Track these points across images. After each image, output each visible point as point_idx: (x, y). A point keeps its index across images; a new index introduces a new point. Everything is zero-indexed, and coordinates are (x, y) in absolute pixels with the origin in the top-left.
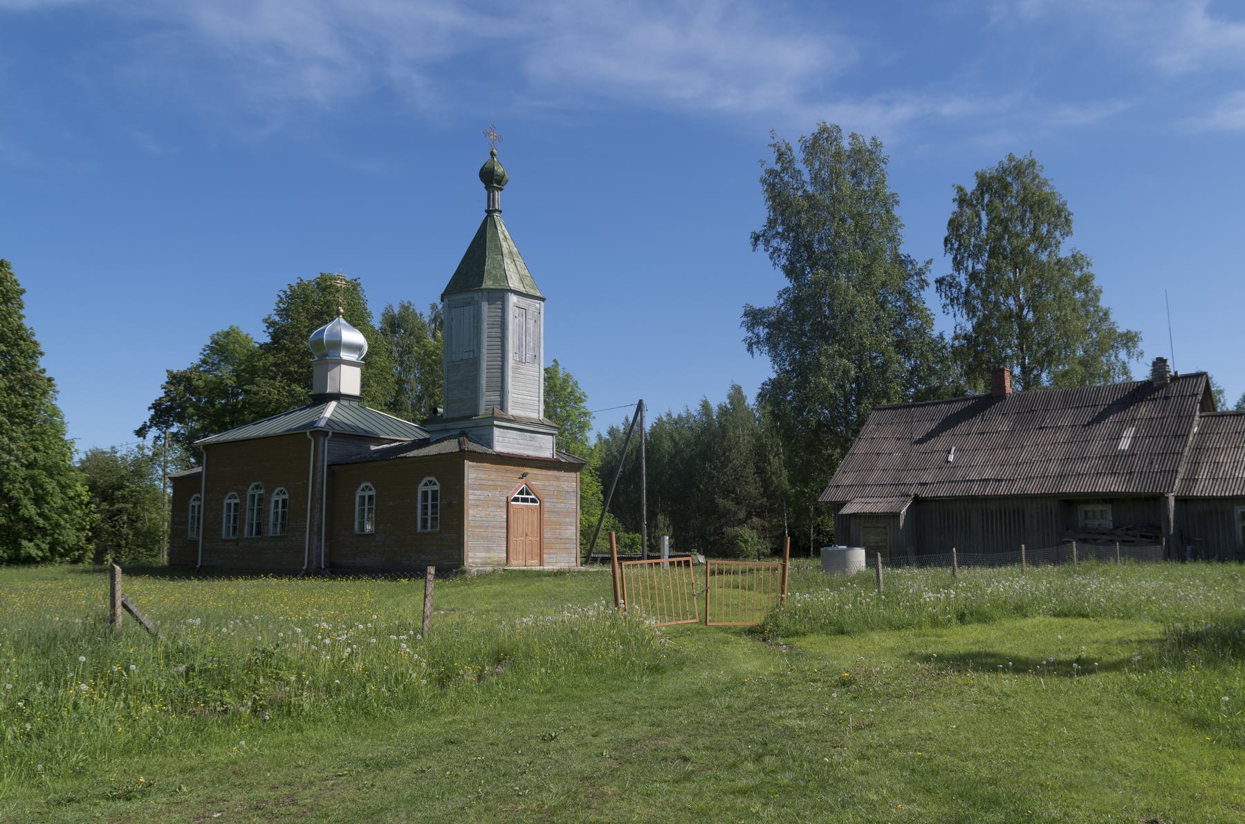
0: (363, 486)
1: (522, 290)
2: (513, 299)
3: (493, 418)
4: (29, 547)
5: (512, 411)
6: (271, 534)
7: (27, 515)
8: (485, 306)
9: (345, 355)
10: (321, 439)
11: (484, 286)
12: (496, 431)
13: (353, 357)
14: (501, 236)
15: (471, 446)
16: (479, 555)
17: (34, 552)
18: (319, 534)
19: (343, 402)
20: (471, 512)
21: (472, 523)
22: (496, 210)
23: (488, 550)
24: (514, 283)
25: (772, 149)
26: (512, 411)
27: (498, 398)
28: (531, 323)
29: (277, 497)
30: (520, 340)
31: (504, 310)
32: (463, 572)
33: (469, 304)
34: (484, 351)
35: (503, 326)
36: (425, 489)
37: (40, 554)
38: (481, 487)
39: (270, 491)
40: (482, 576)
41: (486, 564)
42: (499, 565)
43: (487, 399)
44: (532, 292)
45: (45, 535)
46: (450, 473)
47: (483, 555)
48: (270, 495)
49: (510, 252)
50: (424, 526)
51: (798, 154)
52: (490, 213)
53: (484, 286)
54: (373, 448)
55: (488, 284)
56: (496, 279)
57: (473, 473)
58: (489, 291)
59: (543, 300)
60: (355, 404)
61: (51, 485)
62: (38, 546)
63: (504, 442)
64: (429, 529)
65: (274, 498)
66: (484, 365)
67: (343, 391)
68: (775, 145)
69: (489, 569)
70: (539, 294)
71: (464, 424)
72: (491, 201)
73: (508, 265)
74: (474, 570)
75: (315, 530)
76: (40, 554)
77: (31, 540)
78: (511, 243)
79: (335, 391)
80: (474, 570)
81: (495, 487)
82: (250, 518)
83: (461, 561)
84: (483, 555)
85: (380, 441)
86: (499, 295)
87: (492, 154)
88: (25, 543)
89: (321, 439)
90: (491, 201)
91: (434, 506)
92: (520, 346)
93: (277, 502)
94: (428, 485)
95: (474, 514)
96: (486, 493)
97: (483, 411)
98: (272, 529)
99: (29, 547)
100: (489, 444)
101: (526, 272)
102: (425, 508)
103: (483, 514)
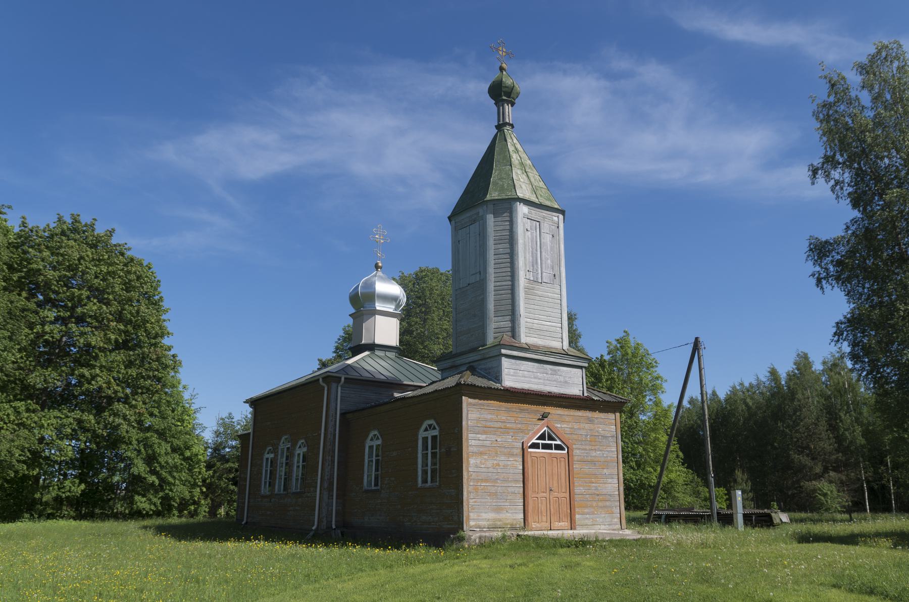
0: (371, 435)
1: (533, 198)
2: (522, 210)
3: (500, 345)
4: (141, 502)
5: (525, 338)
6: (294, 490)
7: (136, 473)
8: (490, 219)
9: (379, 306)
10: (334, 385)
11: (488, 197)
12: (505, 362)
13: (390, 308)
14: (511, 148)
15: (469, 379)
16: (484, 516)
17: (146, 506)
18: (330, 490)
19: (377, 352)
20: (472, 461)
21: (474, 476)
22: (505, 124)
23: (498, 509)
24: (523, 191)
25: (825, 81)
26: (525, 338)
27: (509, 324)
28: (547, 238)
29: (300, 451)
30: (534, 255)
31: (512, 222)
32: (461, 539)
33: (474, 221)
34: (491, 270)
35: (511, 240)
36: (425, 434)
37: (153, 507)
38: (486, 430)
39: (294, 445)
40: (488, 546)
41: (494, 528)
42: (513, 528)
43: (495, 325)
44: (548, 203)
45: (156, 492)
46: (445, 409)
47: (492, 515)
48: (295, 449)
49: (522, 164)
50: (425, 481)
51: (854, 79)
52: (500, 127)
53: (488, 197)
54: (396, 395)
55: (493, 194)
56: (502, 190)
57: (473, 413)
58: (493, 201)
59: (563, 212)
60: (392, 355)
61: (163, 448)
62: (151, 502)
63: (515, 374)
64: (429, 483)
65: (298, 451)
66: (491, 286)
67: (377, 342)
68: (825, 78)
69: (497, 534)
70: (556, 206)
71: (472, 357)
72: (501, 114)
73: (518, 175)
74: (475, 536)
75: (326, 485)
76: (153, 507)
77: (144, 496)
78: (524, 156)
79: (371, 342)
80: (475, 536)
81: (506, 430)
82: (281, 471)
83: (459, 524)
84: (492, 515)
85: (403, 387)
86: (506, 206)
87: (502, 69)
88: (137, 498)
89: (334, 385)
90: (501, 114)
91: (434, 455)
92: (534, 264)
93: (299, 455)
94: (427, 431)
95: (474, 465)
96: (493, 438)
97: (490, 340)
98: (295, 486)
99: (141, 502)
100: (498, 378)
101: (542, 184)
102: (425, 456)
103: (489, 463)
